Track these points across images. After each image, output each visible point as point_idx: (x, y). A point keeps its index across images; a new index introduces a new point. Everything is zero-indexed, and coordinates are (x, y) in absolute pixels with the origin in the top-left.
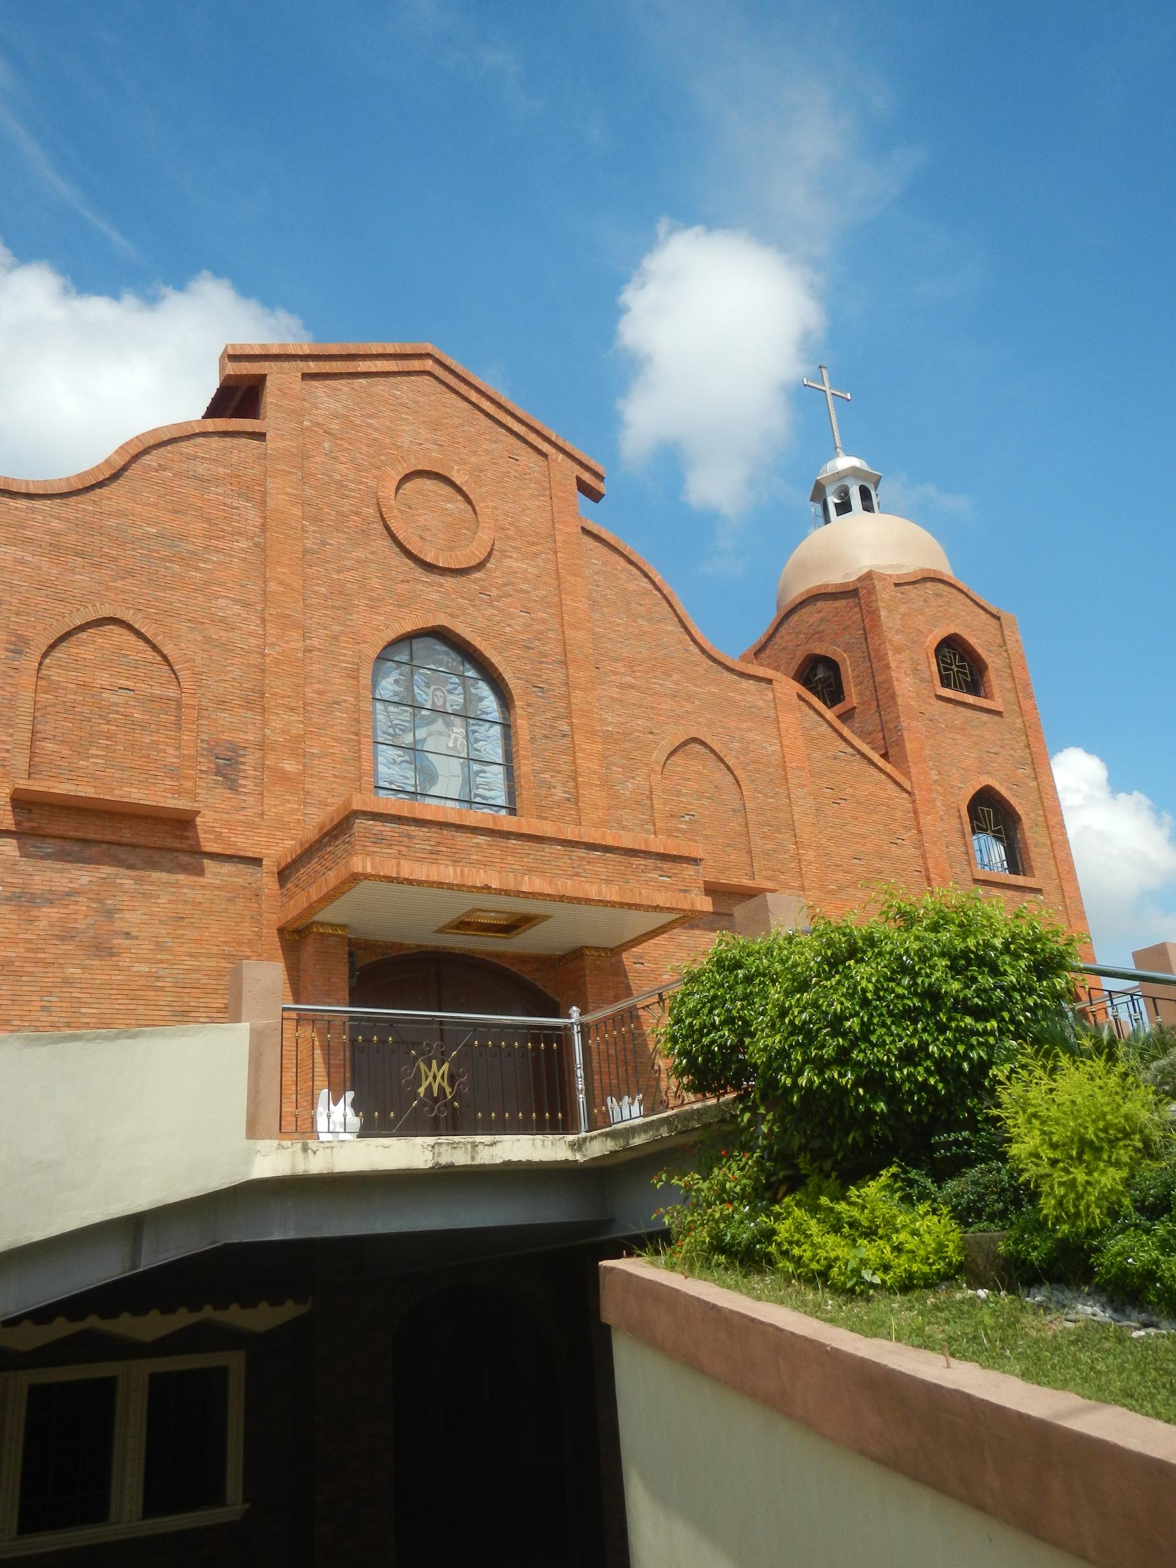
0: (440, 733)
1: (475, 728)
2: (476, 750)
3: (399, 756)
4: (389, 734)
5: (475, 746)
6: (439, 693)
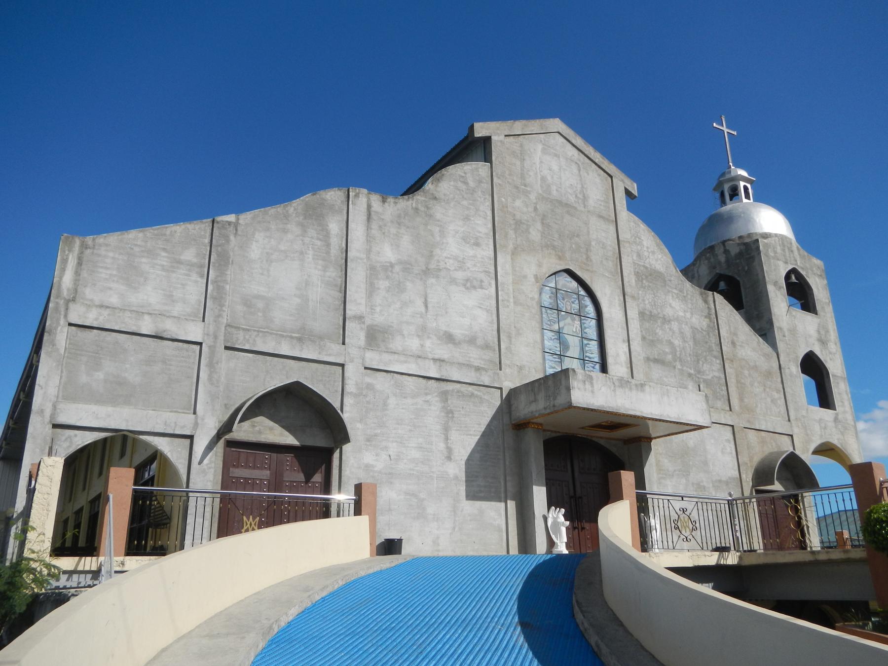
1: (585, 321)
2: (585, 333)
3: (553, 336)
4: (548, 325)
5: (585, 331)
6: (568, 303)
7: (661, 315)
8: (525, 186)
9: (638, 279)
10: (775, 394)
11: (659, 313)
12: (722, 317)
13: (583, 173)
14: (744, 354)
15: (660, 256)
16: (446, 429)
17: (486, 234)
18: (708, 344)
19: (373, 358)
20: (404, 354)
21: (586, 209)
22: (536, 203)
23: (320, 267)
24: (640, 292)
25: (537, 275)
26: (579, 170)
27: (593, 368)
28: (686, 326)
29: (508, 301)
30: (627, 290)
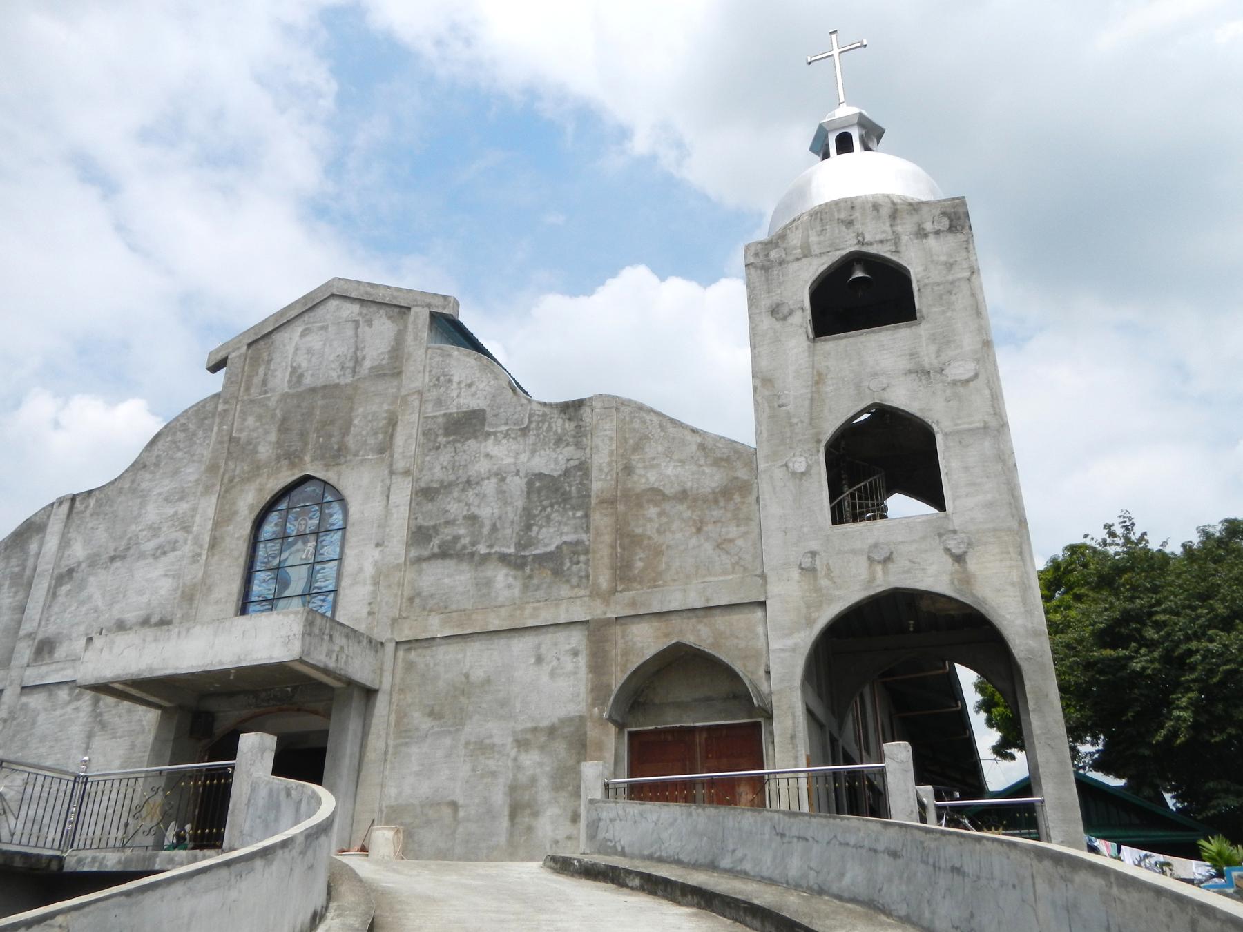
0: (298, 551)
5: (321, 552)
6: (303, 522)
7: (460, 480)
8: (266, 392)
9: (429, 440)
10: (735, 529)
11: (457, 479)
12: (605, 430)
13: (364, 329)
14: (652, 479)
15: (481, 386)
16: (90, 736)
17: (197, 481)
18: (562, 490)
19: (33, 676)
20: (69, 661)
21: (356, 377)
22: (275, 410)
23: (11, 594)
24: (428, 458)
25: (253, 504)
26: (357, 327)
27: (324, 601)
28: (517, 478)
29: (200, 555)
30: (400, 465)
